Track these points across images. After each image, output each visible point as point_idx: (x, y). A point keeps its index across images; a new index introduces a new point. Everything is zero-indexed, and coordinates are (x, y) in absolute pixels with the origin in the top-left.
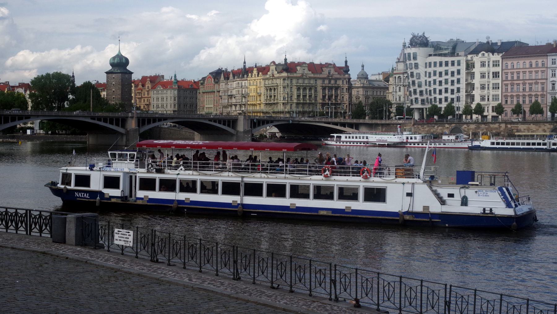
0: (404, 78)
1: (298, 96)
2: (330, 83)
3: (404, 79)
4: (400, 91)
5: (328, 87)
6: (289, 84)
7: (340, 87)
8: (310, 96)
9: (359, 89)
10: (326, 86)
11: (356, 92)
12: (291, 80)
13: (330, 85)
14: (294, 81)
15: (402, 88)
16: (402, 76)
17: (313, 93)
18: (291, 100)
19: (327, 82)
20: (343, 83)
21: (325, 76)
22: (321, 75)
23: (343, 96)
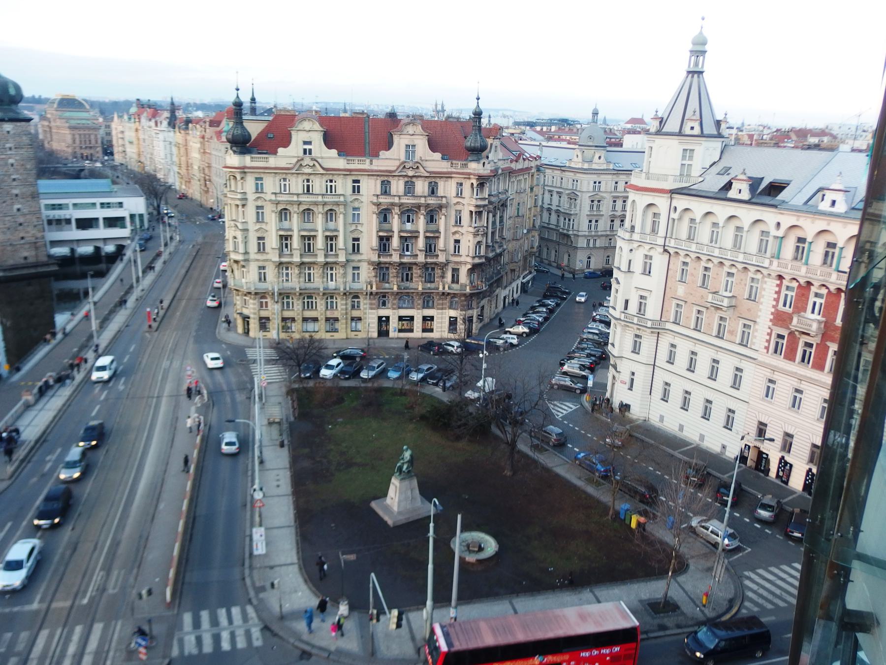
0: (675, 216)
1: (285, 239)
2: (409, 188)
3: (671, 222)
4: (647, 271)
5: (401, 205)
6: (251, 196)
7: (446, 206)
8: (331, 239)
9: (578, 175)
10: (393, 204)
11: (571, 181)
12: (257, 179)
13: (404, 200)
14: (270, 184)
15: (659, 262)
16: (662, 202)
17: (341, 228)
18: (261, 249)
19: (398, 186)
20: (460, 194)
21: (392, 165)
22: (375, 161)
23: (457, 237)
